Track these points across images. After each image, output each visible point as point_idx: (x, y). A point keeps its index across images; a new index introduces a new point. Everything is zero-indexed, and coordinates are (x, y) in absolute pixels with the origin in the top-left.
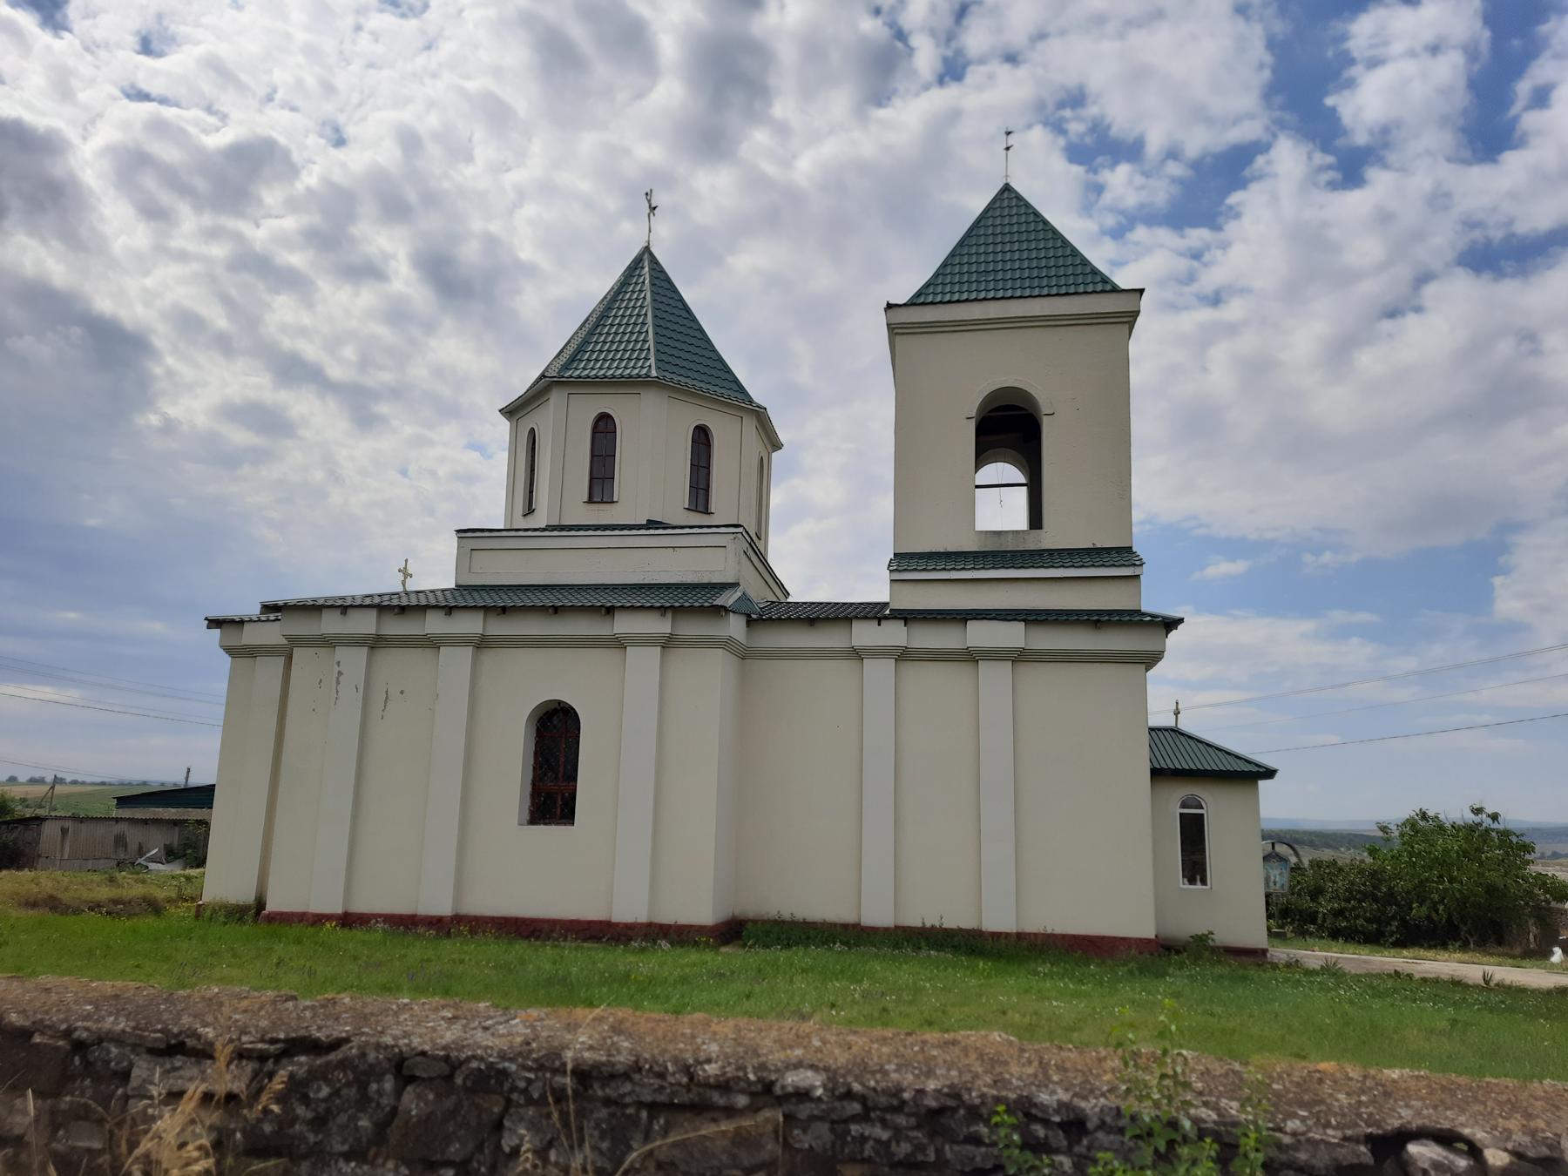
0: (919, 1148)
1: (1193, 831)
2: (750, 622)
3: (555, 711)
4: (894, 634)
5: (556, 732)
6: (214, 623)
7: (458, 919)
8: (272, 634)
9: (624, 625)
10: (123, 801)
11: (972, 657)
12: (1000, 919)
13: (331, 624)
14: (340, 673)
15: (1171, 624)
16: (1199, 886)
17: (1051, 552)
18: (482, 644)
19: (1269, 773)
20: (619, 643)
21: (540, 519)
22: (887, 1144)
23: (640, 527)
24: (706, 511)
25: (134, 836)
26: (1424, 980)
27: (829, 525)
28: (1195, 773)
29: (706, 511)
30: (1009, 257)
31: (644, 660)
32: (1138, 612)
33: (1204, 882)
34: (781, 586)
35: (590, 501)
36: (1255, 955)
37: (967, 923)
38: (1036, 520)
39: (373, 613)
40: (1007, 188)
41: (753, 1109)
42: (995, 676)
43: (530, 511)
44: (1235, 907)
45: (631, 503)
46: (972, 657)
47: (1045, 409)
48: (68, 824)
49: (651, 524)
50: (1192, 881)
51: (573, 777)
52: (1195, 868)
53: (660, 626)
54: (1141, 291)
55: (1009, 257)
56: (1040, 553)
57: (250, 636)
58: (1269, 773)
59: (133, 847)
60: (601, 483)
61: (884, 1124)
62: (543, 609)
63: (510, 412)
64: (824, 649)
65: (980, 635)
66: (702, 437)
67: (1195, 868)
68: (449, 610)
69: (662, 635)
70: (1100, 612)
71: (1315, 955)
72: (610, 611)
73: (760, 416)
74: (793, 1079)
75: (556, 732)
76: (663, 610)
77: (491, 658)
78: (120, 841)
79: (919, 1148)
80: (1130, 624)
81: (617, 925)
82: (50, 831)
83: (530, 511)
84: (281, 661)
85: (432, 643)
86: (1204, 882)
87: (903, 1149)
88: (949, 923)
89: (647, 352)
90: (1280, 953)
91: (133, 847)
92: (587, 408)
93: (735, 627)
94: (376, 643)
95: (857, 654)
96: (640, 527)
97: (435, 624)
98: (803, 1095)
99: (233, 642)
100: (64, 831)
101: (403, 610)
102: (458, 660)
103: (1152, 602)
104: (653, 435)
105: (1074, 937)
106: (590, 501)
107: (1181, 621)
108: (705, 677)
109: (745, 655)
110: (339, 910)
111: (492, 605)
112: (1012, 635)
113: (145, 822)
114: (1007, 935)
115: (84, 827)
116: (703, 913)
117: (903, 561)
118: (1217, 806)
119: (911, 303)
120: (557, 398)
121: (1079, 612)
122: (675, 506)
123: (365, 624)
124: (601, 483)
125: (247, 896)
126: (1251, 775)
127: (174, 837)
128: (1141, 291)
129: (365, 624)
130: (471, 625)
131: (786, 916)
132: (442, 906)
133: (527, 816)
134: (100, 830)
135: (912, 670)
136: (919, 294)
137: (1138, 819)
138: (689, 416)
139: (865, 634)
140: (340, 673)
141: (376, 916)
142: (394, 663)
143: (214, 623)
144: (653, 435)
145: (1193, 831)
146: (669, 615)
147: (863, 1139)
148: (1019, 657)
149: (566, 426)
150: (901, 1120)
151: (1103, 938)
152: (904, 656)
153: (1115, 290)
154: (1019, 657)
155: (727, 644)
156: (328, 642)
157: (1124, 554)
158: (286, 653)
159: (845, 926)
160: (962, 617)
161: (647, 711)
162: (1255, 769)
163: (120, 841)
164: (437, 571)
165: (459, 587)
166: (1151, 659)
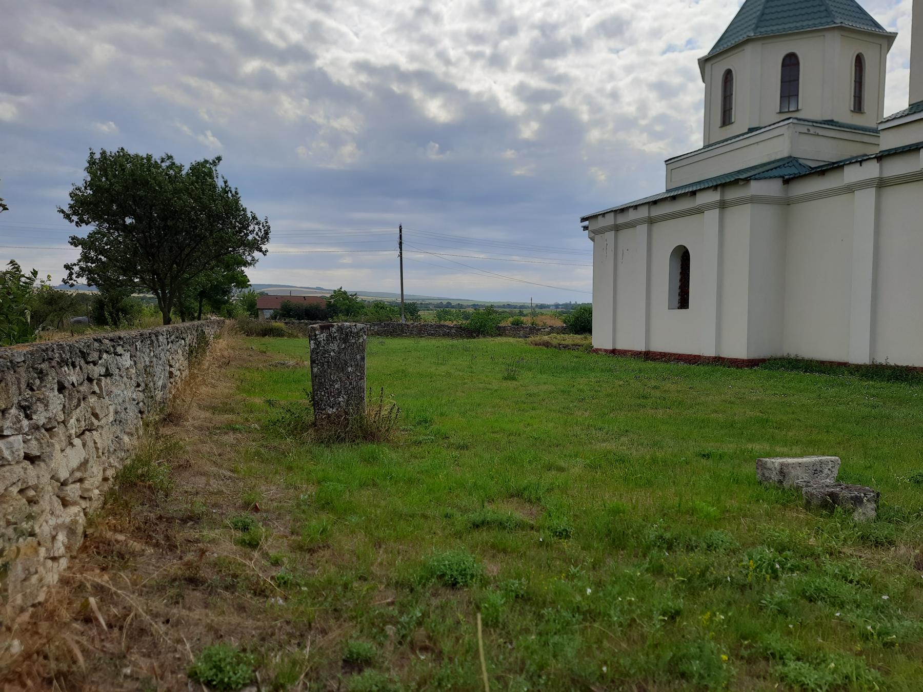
2: (786, 182)
9: (703, 199)
20: (699, 211)
45: (742, 119)
49: (751, 130)
64: (831, 190)
69: (716, 202)
72: (694, 193)
76: (715, 188)
77: (658, 228)
94: (617, 228)
95: (850, 189)
102: (643, 229)
108: (744, 223)
123: (610, 220)
133: (678, 305)
138: (775, 53)
146: (719, 189)
155: (753, 200)
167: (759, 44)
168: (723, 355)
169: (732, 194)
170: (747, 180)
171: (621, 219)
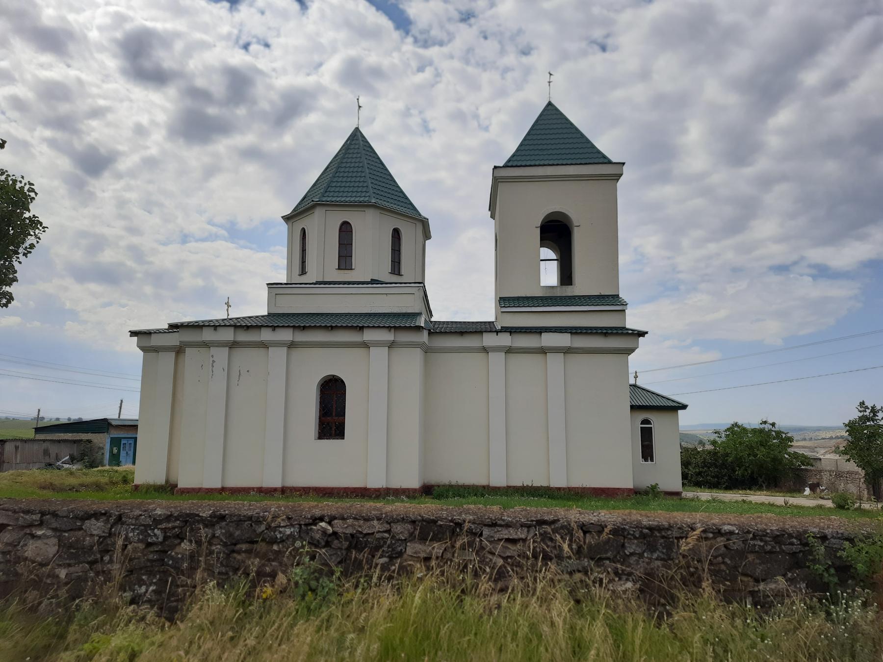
0: (773, 547)
1: (647, 435)
2: (430, 333)
3: (330, 380)
4: (505, 340)
5: (332, 394)
6: (133, 334)
7: (223, 489)
8: (174, 339)
9: (369, 336)
10: (38, 430)
11: (543, 351)
12: (558, 481)
13: (208, 335)
14: (214, 361)
15: (642, 334)
16: (650, 462)
17: (580, 297)
18: (292, 345)
19: (684, 407)
21: (312, 276)
22: (763, 546)
23: (367, 283)
24: (399, 274)
25: (54, 450)
26: (756, 503)
27: (461, 279)
28: (652, 409)
29: (399, 274)
30: (553, 142)
31: (379, 355)
32: (624, 328)
33: (652, 460)
34: (431, 312)
35: (339, 268)
36: (678, 494)
37: (545, 484)
38: (566, 276)
39: (232, 329)
40: (550, 104)
41: (714, 538)
42: (555, 361)
43: (303, 272)
44: (667, 473)
45: (362, 269)
46: (543, 351)
47: (575, 223)
48: (18, 444)
49: (373, 282)
50: (646, 460)
51: (342, 414)
52: (647, 453)
53: (388, 336)
54: (624, 164)
55: (553, 142)
56: (574, 297)
57: (155, 341)
58: (684, 407)
59: (53, 455)
60: (345, 259)
61: (761, 540)
62: (326, 327)
63: (287, 218)
65: (548, 340)
66: (396, 234)
67: (647, 453)
68: (274, 328)
70: (606, 328)
71: (705, 495)
72: (362, 328)
73: (424, 224)
74: (726, 528)
75: (332, 394)
76: (389, 328)
77: (297, 353)
78: (46, 453)
79: (773, 547)
80: (622, 334)
81: (369, 489)
82: (9, 448)
83: (303, 272)
84: (173, 354)
85: (264, 345)
86: (652, 460)
87: (769, 548)
88: (537, 484)
89: (356, 182)
90: (689, 494)
91: (53, 455)
92: (336, 218)
93: (424, 337)
94: (233, 345)
95: (485, 350)
96: (367, 283)
97: (266, 335)
98: (731, 533)
99: (147, 342)
100: (17, 448)
101: (248, 328)
103: (632, 322)
104: (371, 233)
105: (594, 489)
106: (339, 268)
107: (647, 333)
108: (410, 362)
109: (428, 351)
110: (219, 486)
111: (287, 324)
112: (564, 340)
113: (59, 441)
114: (564, 489)
115: (27, 445)
116: (414, 483)
117: (505, 302)
118: (658, 422)
119: (506, 166)
120: (319, 212)
121: (596, 328)
122: (384, 272)
123: (228, 335)
124: (345, 259)
125: (161, 480)
126: (674, 408)
127: (75, 450)
128: (624, 164)
129: (228, 335)
130: (286, 335)
131: (454, 483)
132: (277, 483)
134: (36, 447)
135: (512, 356)
136: (509, 161)
137: (627, 429)
138: (391, 223)
139: (489, 340)
140: (214, 361)
141: (253, 489)
142: (243, 356)
143: (133, 334)
144: (371, 233)
145: (647, 435)
146: (393, 330)
147: (755, 545)
148: (567, 351)
149: (323, 228)
150: (768, 539)
151: (608, 489)
152: (509, 351)
153: (610, 162)
154: (567, 351)
156: (206, 345)
157: (614, 299)
158: (179, 351)
159: (484, 487)
160: (539, 331)
161: (376, 379)
162: (675, 404)
163: (46, 453)
164: (257, 306)
165: (269, 315)
166: (632, 350)
167: (378, 212)
168: (368, 487)
169: (405, 337)
170: (481, 332)
171: (243, 337)
